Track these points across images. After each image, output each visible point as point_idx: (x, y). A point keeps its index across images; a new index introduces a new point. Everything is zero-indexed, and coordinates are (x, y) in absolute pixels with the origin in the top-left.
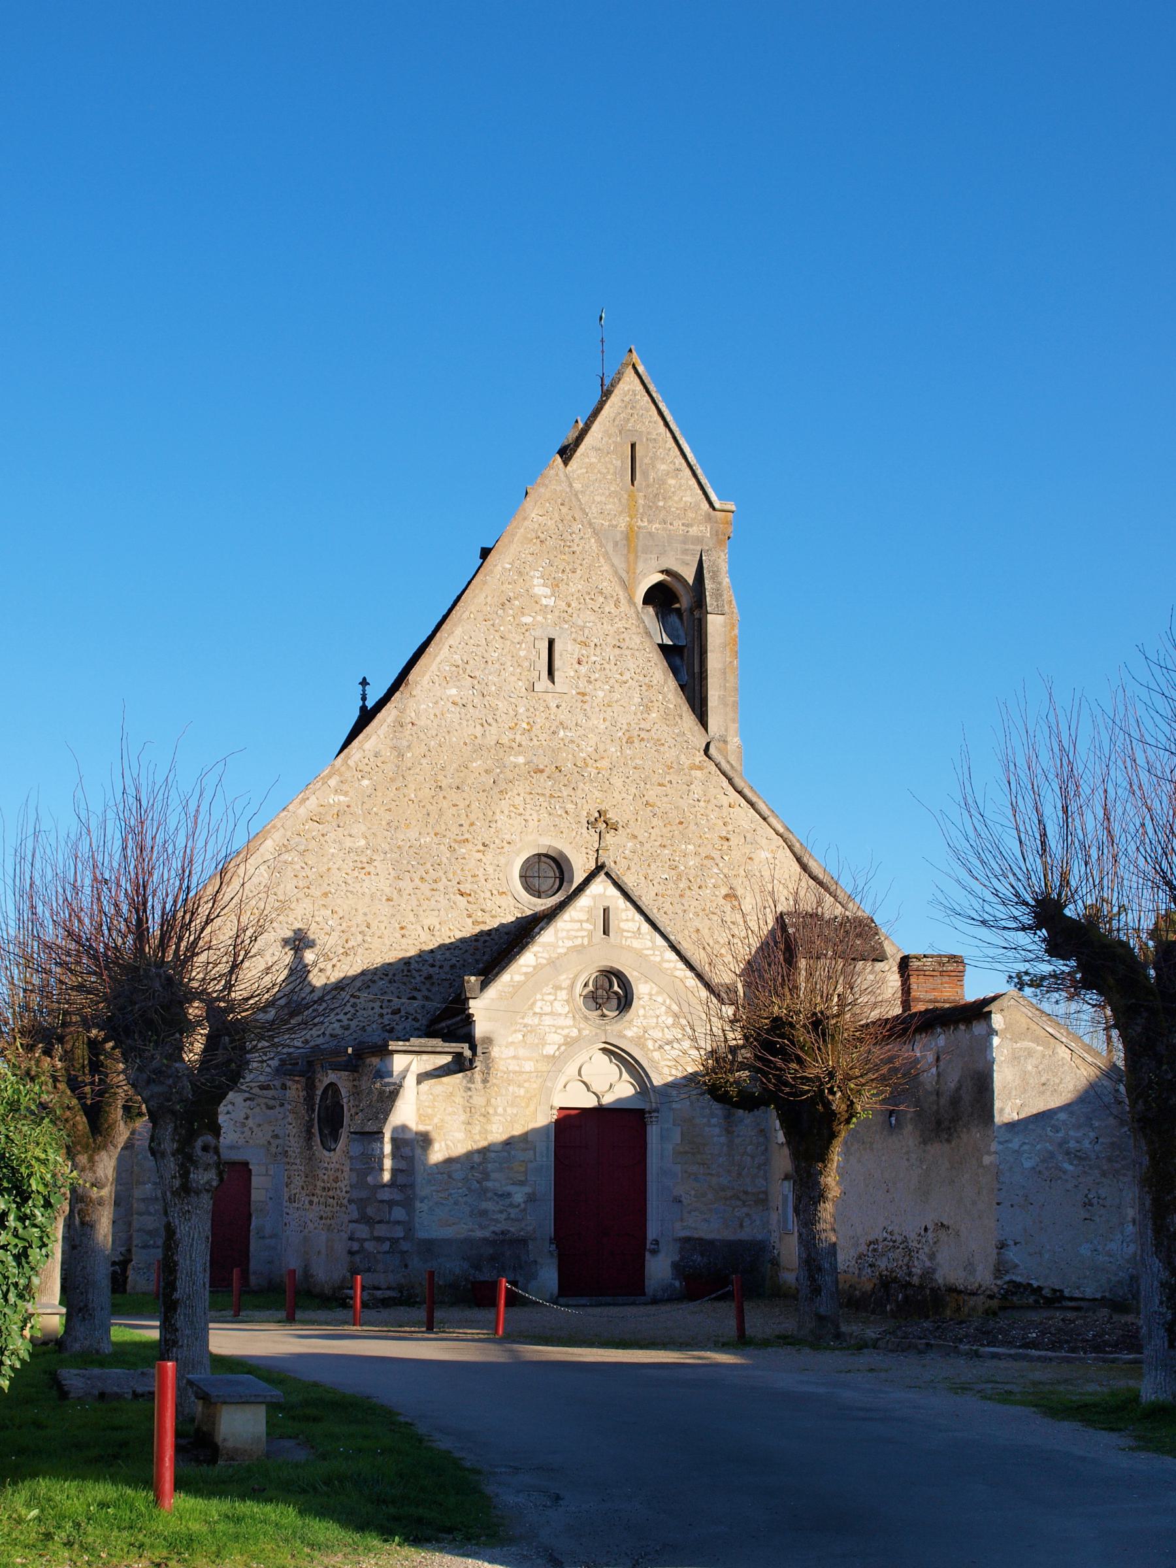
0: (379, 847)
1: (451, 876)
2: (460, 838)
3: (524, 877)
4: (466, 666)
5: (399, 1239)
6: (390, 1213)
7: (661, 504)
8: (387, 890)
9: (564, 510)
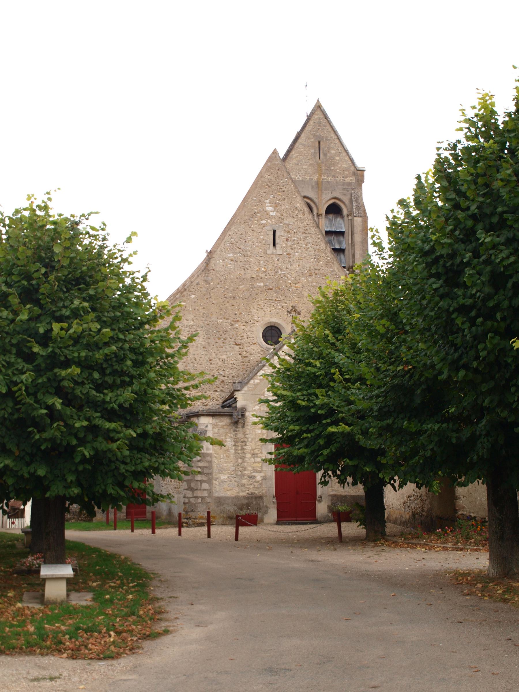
6: (201, 485)
7: (332, 168)
8: (204, 343)
9: (279, 172)
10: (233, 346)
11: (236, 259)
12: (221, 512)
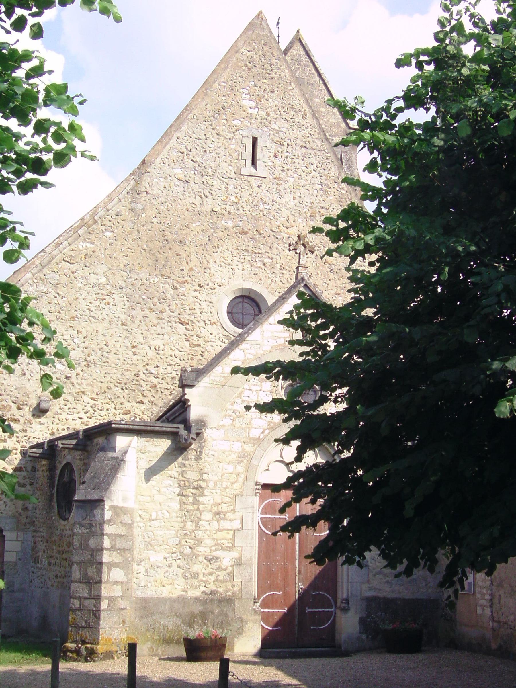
0: (117, 284)
1: (173, 308)
2: (181, 279)
3: (230, 313)
4: (190, 153)
5: (117, 597)
8: (123, 317)
9: (266, 48)
10: (174, 325)
11: (187, 179)
12: (148, 630)
